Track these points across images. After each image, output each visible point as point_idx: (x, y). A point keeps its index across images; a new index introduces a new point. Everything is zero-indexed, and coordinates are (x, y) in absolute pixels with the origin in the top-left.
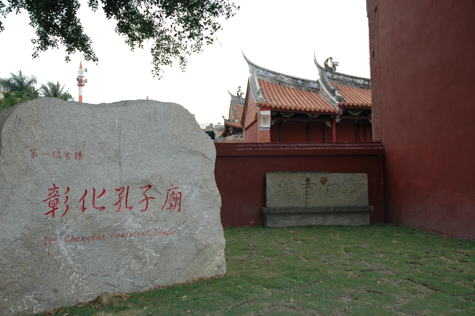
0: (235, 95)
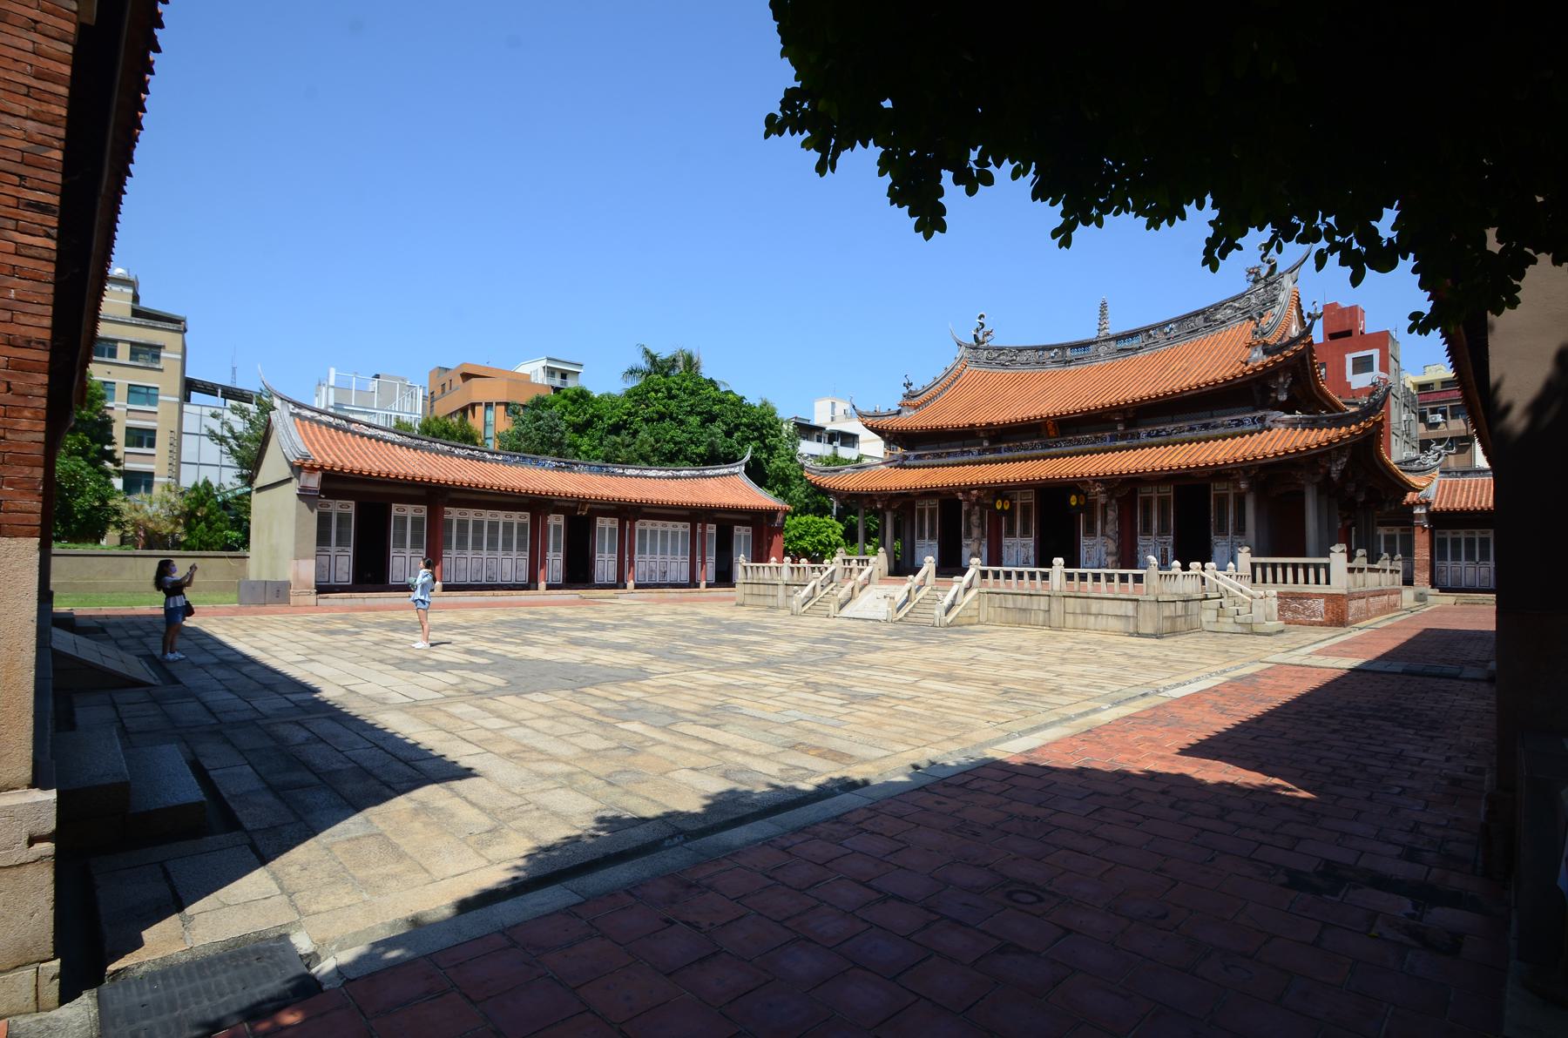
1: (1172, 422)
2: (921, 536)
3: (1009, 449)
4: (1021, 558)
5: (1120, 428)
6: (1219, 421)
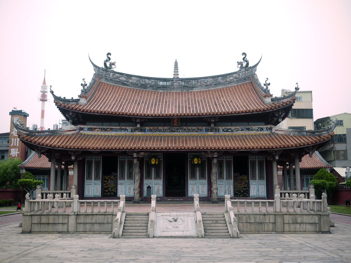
0: (102, 65)
1: (232, 125)
2: (89, 178)
3: (151, 130)
5: (212, 125)
6: (254, 127)
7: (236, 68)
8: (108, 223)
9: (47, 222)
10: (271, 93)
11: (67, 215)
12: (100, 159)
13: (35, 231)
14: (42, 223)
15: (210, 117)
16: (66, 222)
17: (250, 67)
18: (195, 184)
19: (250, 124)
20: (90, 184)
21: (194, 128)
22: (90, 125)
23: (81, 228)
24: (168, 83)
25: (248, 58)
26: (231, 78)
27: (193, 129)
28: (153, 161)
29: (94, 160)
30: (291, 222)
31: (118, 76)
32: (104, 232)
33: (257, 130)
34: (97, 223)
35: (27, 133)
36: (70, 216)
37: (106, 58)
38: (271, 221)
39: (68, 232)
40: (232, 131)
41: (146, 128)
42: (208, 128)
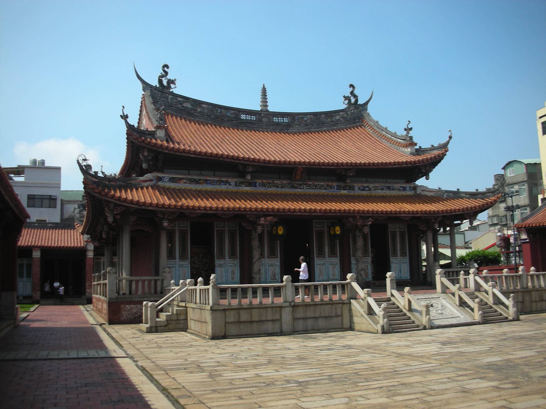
0: (154, 82)
3: (263, 185)
4: (270, 274)
7: (341, 105)
8: (337, 316)
9: (249, 320)
10: (415, 140)
11: (278, 307)
12: (187, 227)
13: (231, 334)
14: (244, 322)
15: (345, 169)
16: (277, 317)
17: (360, 105)
18: (324, 264)
19: (388, 180)
20: (173, 267)
21: (322, 184)
22: (172, 173)
23: (300, 325)
24: (254, 118)
25: (356, 92)
26: (338, 118)
27: (322, 185)
28: (280, 230)
29: (177, 229)
30: (538, 300)
31: (180, 101)
32: (332, 329)
33: (399, 190)
34: (322, 317)
35: (96, 180)
36: (283, 310)
37: (160, 72)
38: (520, 300)
39: (281, 333)
40: (370, 190)
41: (257, 181)
42: (340, 184)
